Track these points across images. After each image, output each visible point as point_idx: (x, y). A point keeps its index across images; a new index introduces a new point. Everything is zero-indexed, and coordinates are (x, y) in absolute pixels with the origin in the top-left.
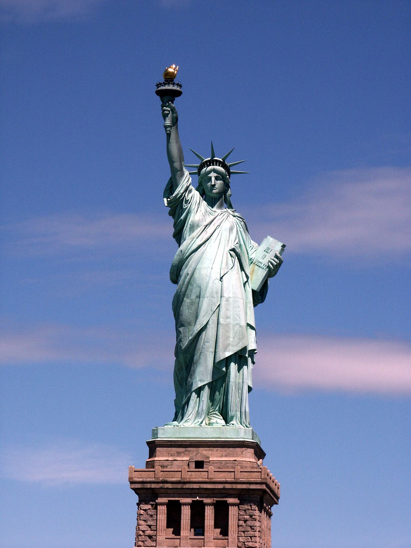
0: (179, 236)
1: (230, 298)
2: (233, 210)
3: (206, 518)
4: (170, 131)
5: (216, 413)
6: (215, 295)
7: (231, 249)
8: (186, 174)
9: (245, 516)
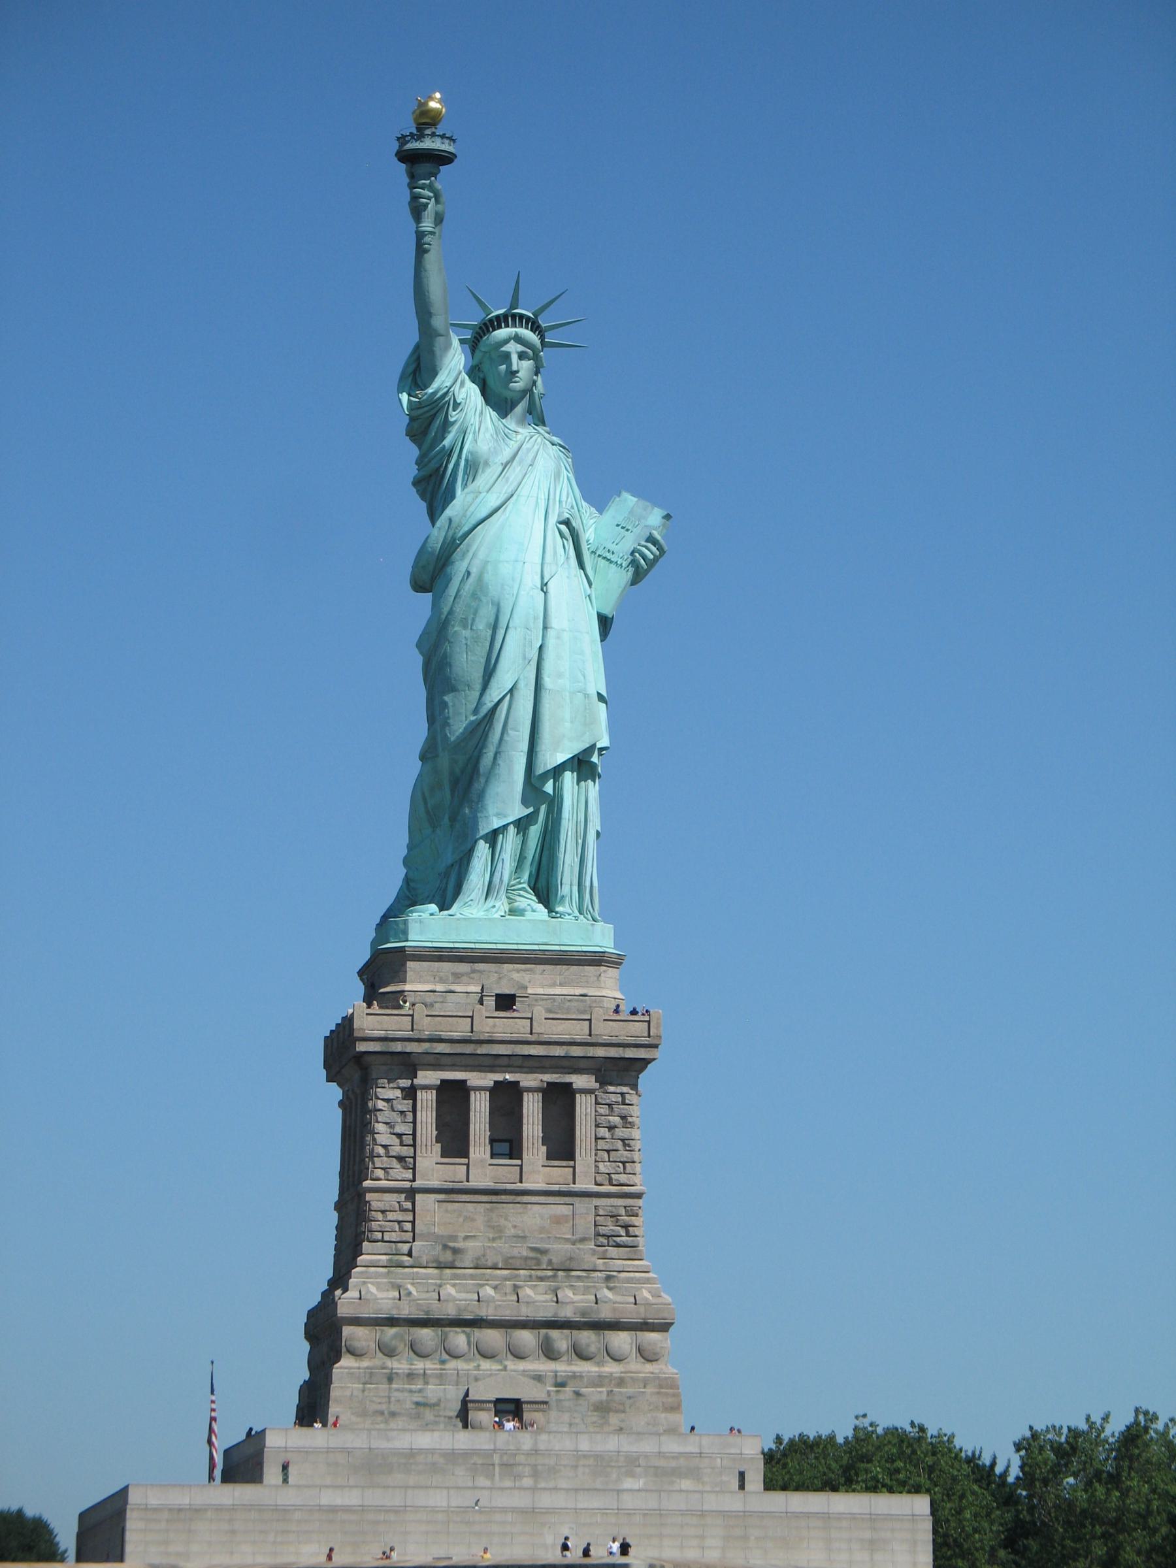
1: (564, 630)
2: (547, 429)
3: (525, 1121)
4: (430, 244)
5: (525, 888)
6: (532, 625)
7: (561, 519)
9: (609, 1117)
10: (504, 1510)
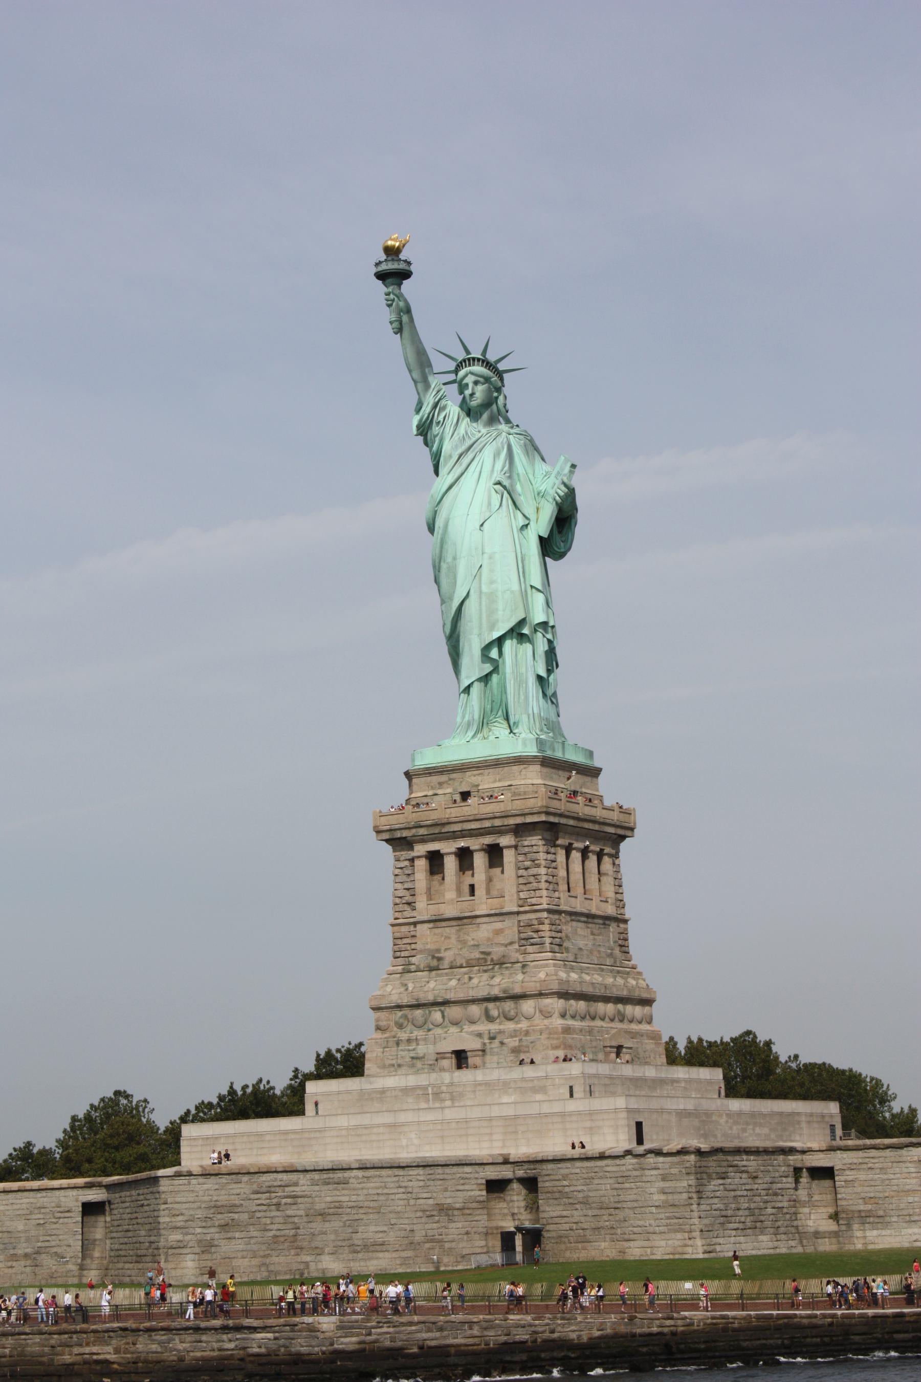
0: (437, 473)
1: (495, 553)
8: (433, 386)
10: (378, 1126)
